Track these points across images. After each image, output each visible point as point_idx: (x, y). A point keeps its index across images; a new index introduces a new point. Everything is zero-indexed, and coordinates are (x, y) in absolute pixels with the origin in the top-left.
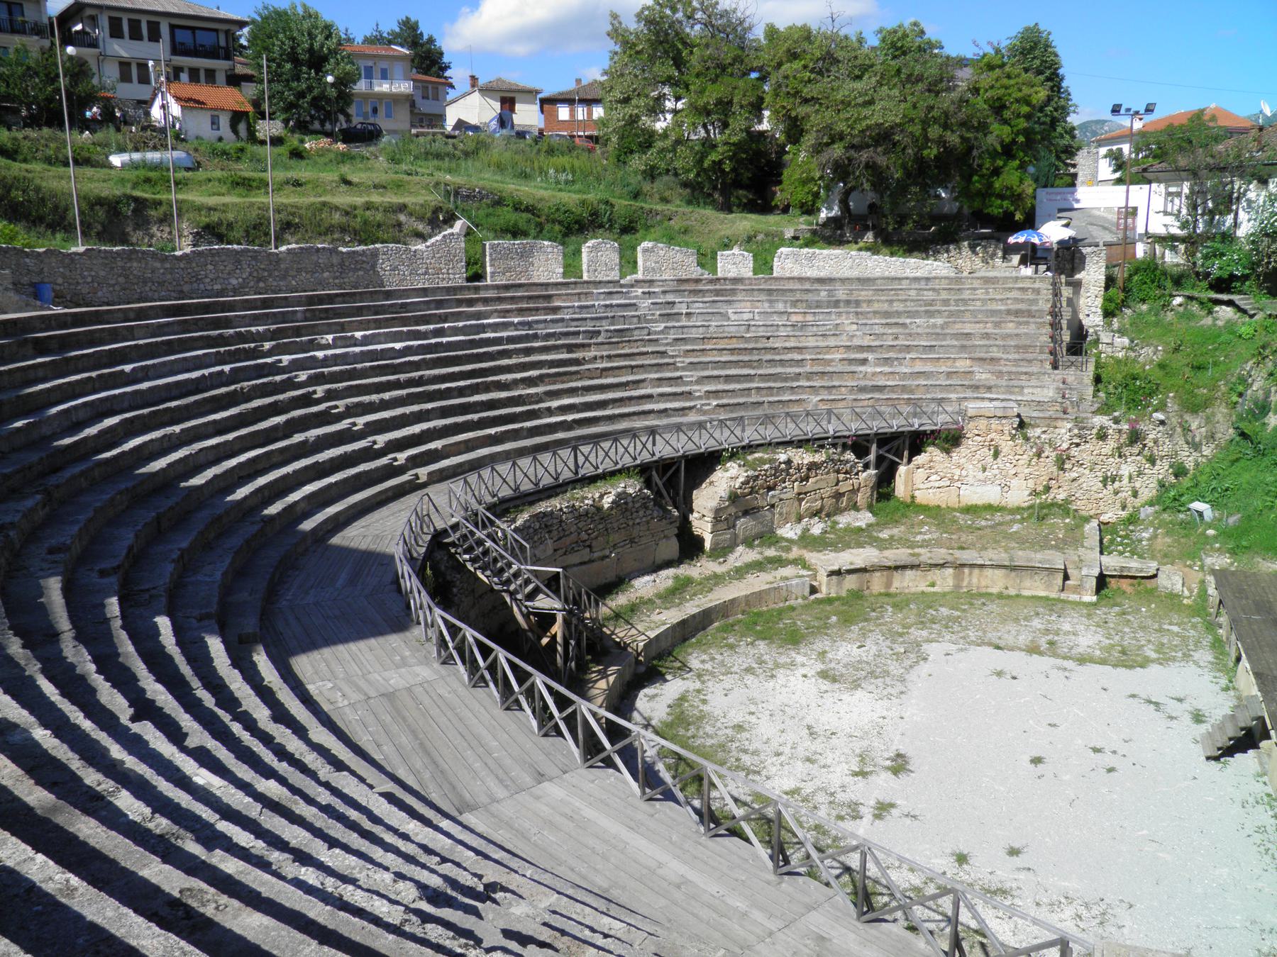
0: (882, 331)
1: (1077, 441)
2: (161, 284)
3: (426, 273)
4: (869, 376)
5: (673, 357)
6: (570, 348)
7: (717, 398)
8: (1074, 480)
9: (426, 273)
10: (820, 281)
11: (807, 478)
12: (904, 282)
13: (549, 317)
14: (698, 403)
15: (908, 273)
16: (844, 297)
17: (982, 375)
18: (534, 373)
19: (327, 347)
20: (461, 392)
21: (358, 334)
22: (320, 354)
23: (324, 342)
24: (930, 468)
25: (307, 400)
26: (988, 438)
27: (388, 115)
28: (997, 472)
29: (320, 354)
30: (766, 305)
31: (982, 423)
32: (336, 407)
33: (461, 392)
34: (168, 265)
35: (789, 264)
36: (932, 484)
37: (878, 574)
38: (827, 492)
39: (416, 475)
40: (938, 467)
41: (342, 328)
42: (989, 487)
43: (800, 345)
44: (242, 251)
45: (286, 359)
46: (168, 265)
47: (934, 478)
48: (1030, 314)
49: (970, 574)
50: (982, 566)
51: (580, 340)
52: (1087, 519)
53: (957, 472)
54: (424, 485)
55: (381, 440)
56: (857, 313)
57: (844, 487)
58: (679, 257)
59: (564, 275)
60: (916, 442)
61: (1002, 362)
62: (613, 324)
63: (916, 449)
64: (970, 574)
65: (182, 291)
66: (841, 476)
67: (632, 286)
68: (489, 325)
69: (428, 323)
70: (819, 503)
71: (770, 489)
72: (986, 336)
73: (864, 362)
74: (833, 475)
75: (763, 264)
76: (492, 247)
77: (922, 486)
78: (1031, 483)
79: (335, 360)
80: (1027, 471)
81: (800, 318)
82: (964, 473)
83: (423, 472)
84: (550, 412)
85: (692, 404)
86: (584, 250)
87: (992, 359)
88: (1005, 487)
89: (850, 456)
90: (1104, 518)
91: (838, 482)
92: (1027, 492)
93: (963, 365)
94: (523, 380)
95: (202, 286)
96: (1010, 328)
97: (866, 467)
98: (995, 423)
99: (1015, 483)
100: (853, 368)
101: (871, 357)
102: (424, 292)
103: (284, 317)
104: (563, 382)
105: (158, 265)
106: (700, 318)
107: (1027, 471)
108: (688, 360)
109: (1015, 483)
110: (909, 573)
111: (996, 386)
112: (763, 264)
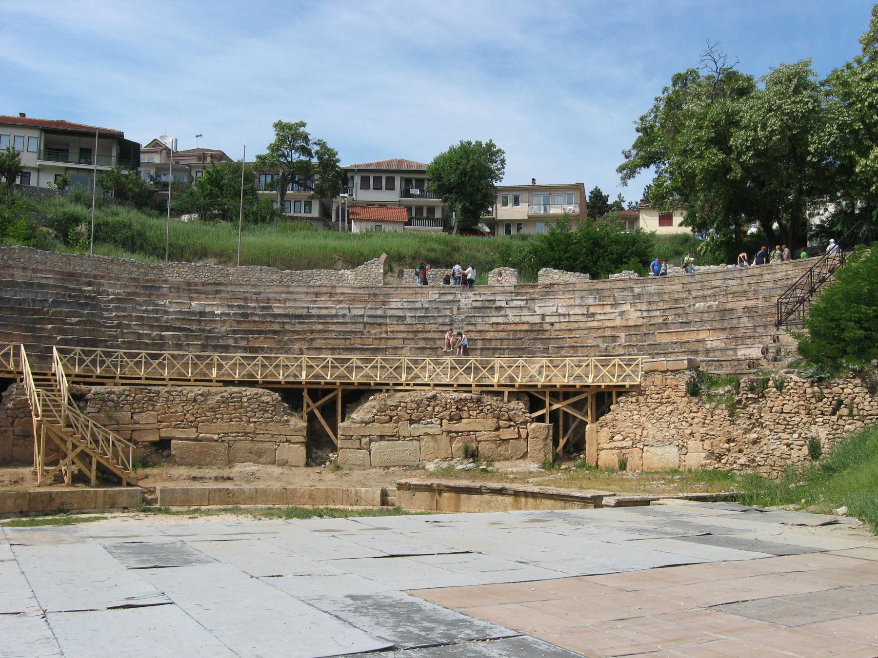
8: (755, 442)
31: (658, 378)
34: (142, 270)
37: (446, 495)
40: (620, 426)
42: (668, 448)
46: (142, 270)
47: (618, 437)
53: (639, 431)
60: (603, 400)
66: (501, 423)
71: (411, 421)
80: (701, 430)
89: (518, 406)
91: (498, 429)
92: (703, 455)
97: (541, 419)
98: (671, 380)
99: (691, 443)
105: (135, 269)
107: (701, 430)
109: (691, 443)
110: (476, 497)
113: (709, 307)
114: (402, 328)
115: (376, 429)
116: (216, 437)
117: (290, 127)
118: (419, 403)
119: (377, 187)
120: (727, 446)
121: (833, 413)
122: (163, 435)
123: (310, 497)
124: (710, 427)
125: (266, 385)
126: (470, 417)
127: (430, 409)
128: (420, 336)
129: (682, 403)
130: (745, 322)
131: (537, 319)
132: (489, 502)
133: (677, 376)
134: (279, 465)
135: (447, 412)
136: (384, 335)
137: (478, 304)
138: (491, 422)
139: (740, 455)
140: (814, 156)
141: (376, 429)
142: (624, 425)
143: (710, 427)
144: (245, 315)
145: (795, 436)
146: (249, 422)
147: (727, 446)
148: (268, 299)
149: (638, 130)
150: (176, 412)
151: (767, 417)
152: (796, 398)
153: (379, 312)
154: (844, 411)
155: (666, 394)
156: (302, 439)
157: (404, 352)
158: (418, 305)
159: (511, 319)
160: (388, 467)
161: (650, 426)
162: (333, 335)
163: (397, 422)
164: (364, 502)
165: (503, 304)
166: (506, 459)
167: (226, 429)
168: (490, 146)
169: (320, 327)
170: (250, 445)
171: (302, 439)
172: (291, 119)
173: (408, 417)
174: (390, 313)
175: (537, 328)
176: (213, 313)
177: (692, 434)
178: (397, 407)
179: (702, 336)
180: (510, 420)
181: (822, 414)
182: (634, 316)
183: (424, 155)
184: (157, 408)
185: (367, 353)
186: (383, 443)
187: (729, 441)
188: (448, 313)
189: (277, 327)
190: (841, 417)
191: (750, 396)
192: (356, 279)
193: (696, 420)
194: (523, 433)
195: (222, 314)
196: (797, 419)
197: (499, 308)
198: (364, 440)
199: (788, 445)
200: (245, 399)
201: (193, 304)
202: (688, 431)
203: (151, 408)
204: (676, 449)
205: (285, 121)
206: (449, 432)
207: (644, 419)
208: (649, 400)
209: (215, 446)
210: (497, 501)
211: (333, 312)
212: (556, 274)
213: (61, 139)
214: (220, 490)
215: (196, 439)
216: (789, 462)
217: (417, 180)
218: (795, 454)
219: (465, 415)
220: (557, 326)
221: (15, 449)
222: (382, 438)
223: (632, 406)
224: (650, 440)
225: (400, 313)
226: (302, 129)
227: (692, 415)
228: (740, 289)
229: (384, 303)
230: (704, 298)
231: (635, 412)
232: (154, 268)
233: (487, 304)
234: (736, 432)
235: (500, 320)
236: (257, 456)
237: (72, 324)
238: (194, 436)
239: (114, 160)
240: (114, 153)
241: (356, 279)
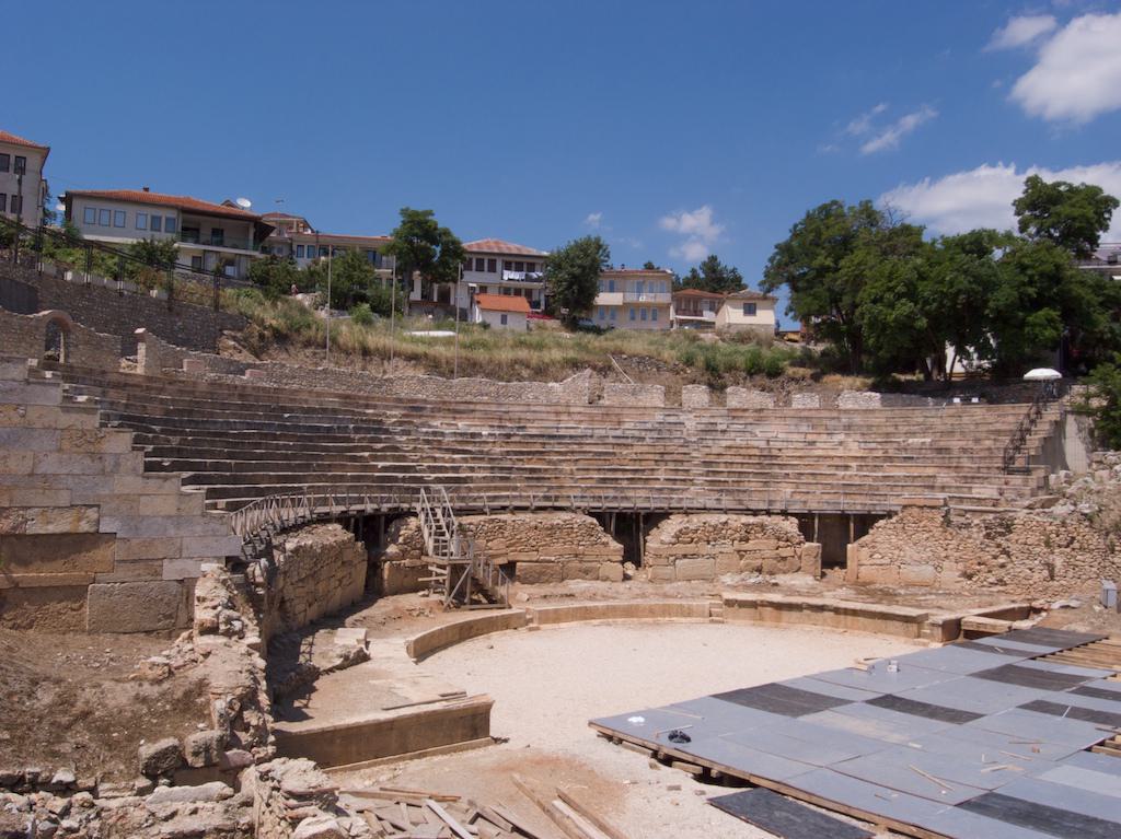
8: (1003, 566)
24: (874, 547)
26: (921, 525)
27: (654, 319)
30: (793, 427)
36: (875, 561)
53: (897, 552)
63: (862, 531)
66: (781, 544)
73: (847, 467)
77: (865, 562)
78: (961, 566)
80: (956, 554)
82: (902, 554)
92: (957, 574)
98: (927, 513)
99: (946, 564)
101: (854, 464)
111: (950, 487)
113: (923, 443)
114: (645, 449)
115: (681, 549)
116: (553, 559)
117: (417, 214)
118: (715, 527)
119: (480, 269)
121: (1067, 546)
122: (511, 559)
126: (757, 538)
127: (724, 532)
128: (667, 457)
129: (937, 532)
130: (966, 463)
131: (763, 444)
134: (603, 580)
135: (738, 535)
136: (634, 457)
137: (703, 427)
138: (773, 542)
139: (989, 575)
140: (991, 312)
141: (681, 549)
144: (508, 436)
145: (1036, 562)
147: (978, 567)
148: (520, 419)
149: (776, 247)
151: (1013, 548)
153: (619, 433)
154: (1076, 545)
155: (921, 525)
156: (621, 559)
157: (659, 472)
158: (649, 426)
159: (738, 442)
162: (589, 456)
163: (696, 543)
165: (724, 427)
166: (785, 573)
167: (562, 552)
168: (598, 239)
169: (575, 447)
170: (579, 565)
171: (621, 559)
172: (418, 206)
174: (628, 433)
175: (765, 453)
176: (480, 435)
177: (946, 557)
179: (930, 471)
180: (787, 541)
181: (1060, 546)
182: (854, 448)
183: (541, 247)
184: (506, 535)
185: (512, 445)
186: (686, 560)
187: (979, 564)
188: (678, 434)
189: (538, 448)
190: (1073, 549)
191: (999, 530)
193: (950, 546)
194: (799, 551)
195: (490, 434)
196: (1038, 550)
197: (724, 432)
198: (672, 558)
199: (1031, 569)
200: (576, 526)
201: (460, 424)
202: (943, 555)
203: (500, 535)
205: (412, 208)
206: (739, 551)
211: (579, 432)
213: (195, 222)
214: (581, 608)
215: (537, 562)
216: (1031, 582)
217: (517, 263)
218: (1036, 576)
220: (785, 453)
221: (406, 579)
222: (685, 556)
223: (890, 532)
224: (907, 559)
225: (637, 433)
226: (430, 218)
228: (943, 428)
229: (619, 423)
230: (913, 434)
232: (386, 380)
233: (710, 427)
235: (729, 443)
236: (586, 573)
237: (378, 451)
238: (535, 559)
239: (251, 244)
240: (251, 237)
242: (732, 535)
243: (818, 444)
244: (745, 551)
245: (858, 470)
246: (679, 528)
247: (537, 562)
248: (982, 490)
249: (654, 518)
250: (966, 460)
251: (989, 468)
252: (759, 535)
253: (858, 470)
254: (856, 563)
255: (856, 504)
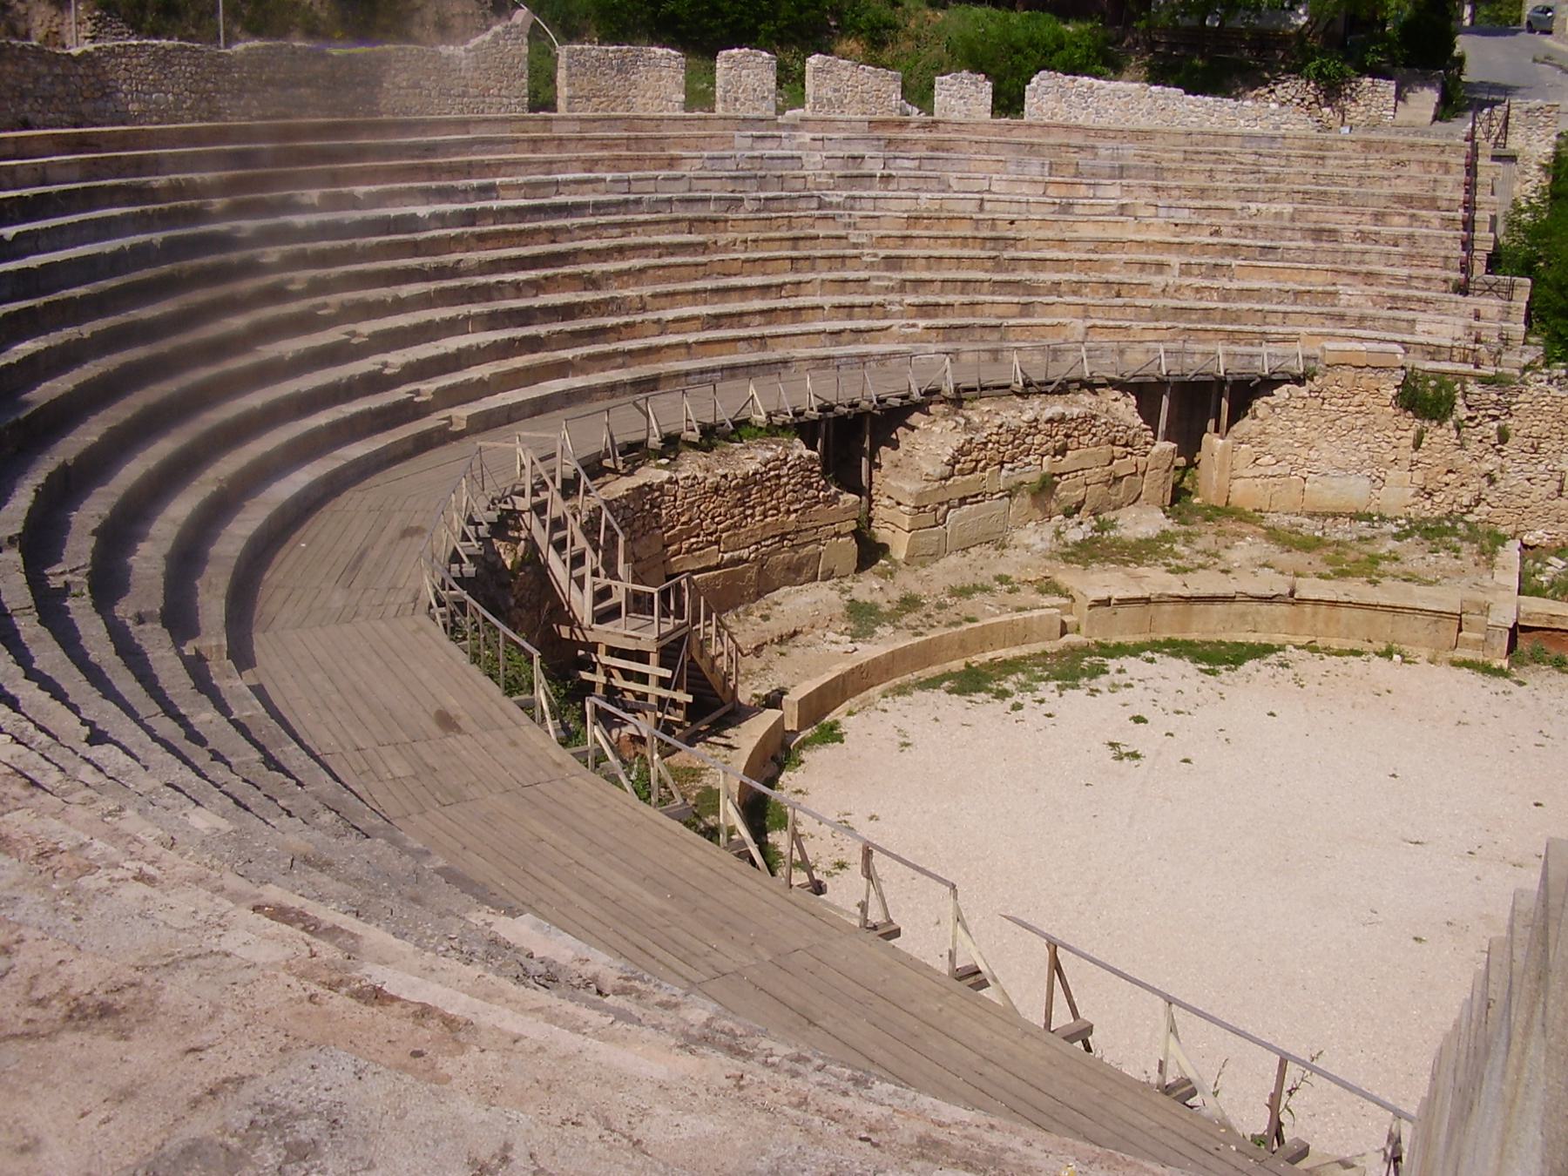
0: (1195, 219)
1: (1496, 413)
2: (48, 100)
3: (464, 94)
4: (1171, 290)
5: (855, 246)
6: (693, 224)
7: (929, 316)
9: (464, 94)
10: (1102, 133)
11: (1062, 451)
12: (1235, 141)
13: (663, 174)
14: (896, 323)
15: (1242, 126)
16: (1135, 162)
17: (1353, 296)
18: (637, 263)
19: (312, 209)
20: (518, 289)
21: (360, 190)
22: (299, 220)
23: (306, 200)
25: (278, 294)
28: (1366, 455)
29: (299, 220)
30: (1012, 168)
32: (325, 306)
33: (518, 289)
35: (1049, 103)
37: (1168, 608)
38: (1097, 474)
39: (449, 418)
41: (335, 179)
42: (1352, 480)
43: (1068, 235)
44: (175, 49)
45: (248, 225)
46: (58, 70)
48: (1432, 204)
49: (1314, 615)
50: (1334, 604)
51: (711, 211)
52: (1502, 540)
53: (1304, 452)
54: (459, 436)
55: (397, 359)
56: (1156, 189)
57: (1122, 467)
58: (873, 83)
59: (688, 106)
61: (1386, 280)
62: (760, 189)
64: (1314, 615)
65: (80, 114)
66: (1118, 450)
67: (794, 127)
68: (567, 183)
69: (469, 176)
70: (1080, 493)
72: (1363, 237)
73: (1161, 267)
74: (1105, 449)
75: (1008, 102)
76: (571, 55)
77: (1246, 473)
78: (1418, 477)
79: (323, 231)
81: (1063, 190)
82: (1313, 454)
83: (461, 414)
84: (663, 327)
85: (886, 323)
86: (721, 65)
87: (1369, 274)
88: (1378, 481)
90: (1529, 539)
92: (1412, 491)
93: (1318, 282)
94: (619, 274)
95: (110, 105)
96: (1398, 225)
99: (1393, 474)
100: (1145, 279)
101: (1175, 260)
102: (464, 124)
103: (242, 159)
104: (681, 280)
105: (43, 69)
106: (905, 184)
108: (882, 253)
111: (1374, 319)
112: (1008, 102)
116: (745, 553)
120: (1446, 479)
123: (961, 647)
124: (1427, 453)
125: (772, 430)
127: (1028, 440)
132: (1243, 615)
133: (1381, 375)
142: (1281, 441)
143: (1427, 453)
145: (1541, 467)
146: (788, 512)
150: (691, 520)
152: (1550, 418)
160: (966, 549)
161: (1325, 445)
163: (984, 469)
164: (1036, 637)
173: (998, 458)
178: (985, 444)
180: (1125, 445)
187: (1450, 471)
192: (476, 69)
204: (1367, 481)
207: (1314, 434)
208: (1326, 406)
209: (746, 570)
210: (1258, 612)
212: (845, 69)
215: (717, 567)
216: (1527, 502)
219: (1073, 443)
222: (963, 501)
223: (1295, 413)
224: (1323, 466)
227: (1399, 433)
231: (1300, 423)
234: (1462, 458)
241: (476, 69)
242: (1041, 445)
243: (1078, 210)
244: (1060, 475)
245: (1182, 273)
246: (956, 445)
247: (717, 567)
248: (1433, 328)
249: (887, 421)
250: (1374, 257)
251: (1428, 279)
252: (1085, 439)
253: (1182, 273)
254: (1227, 476)
255: (1218, 357)
